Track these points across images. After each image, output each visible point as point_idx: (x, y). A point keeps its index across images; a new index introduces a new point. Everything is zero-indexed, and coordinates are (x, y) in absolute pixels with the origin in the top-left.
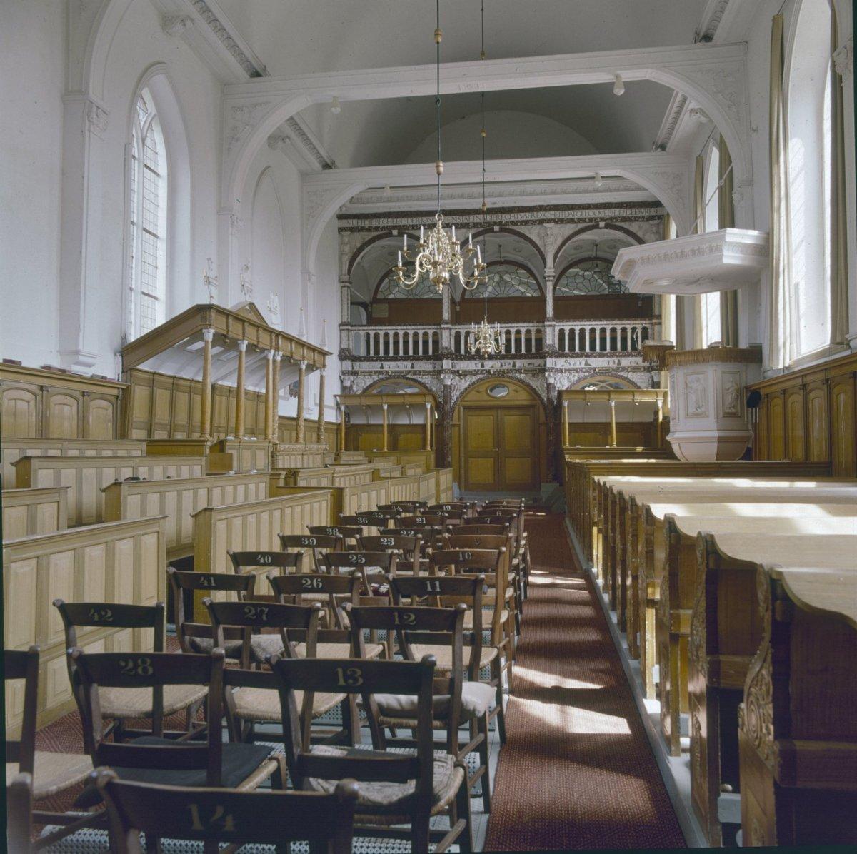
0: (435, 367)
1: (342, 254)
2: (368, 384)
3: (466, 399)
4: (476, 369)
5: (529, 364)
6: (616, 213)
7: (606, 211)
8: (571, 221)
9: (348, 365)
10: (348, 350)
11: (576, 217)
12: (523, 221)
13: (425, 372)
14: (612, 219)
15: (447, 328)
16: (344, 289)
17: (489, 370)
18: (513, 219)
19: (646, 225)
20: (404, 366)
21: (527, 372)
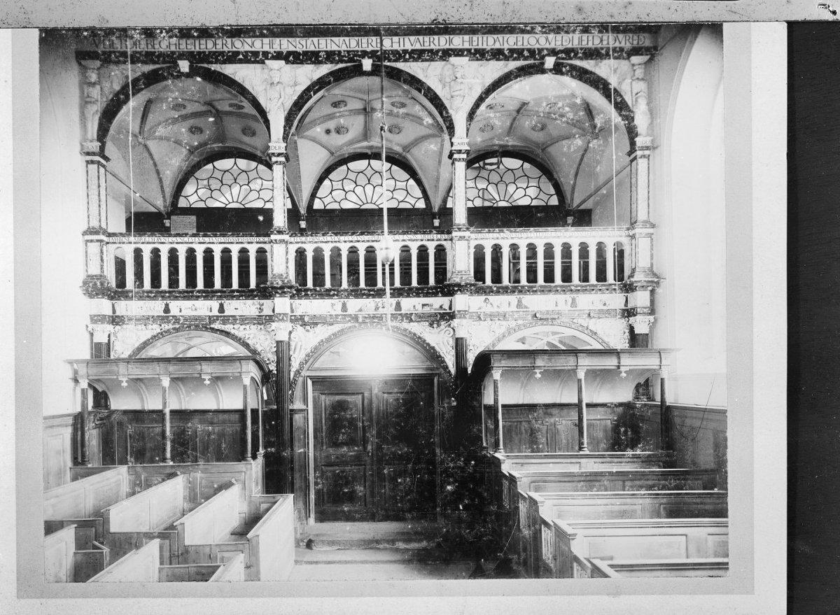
0: (261, 310)
1: (87, 103)
2: (143, 339)
3: (316, 365)
4: (334, 313)
5: (423, 305)
6: (576, 42)
7: (559, 37)
8: (497, 54)
9: (104, 306)
10: (101, 277)
11: (506, 47)
12: (413, 51)
13: (244, 320)
14: (569, 52)
15: (282, 241)
16: (90, 166)
18: (396, 47)
19: (624, 65)
20: (204, 308)
21: (421, 318)
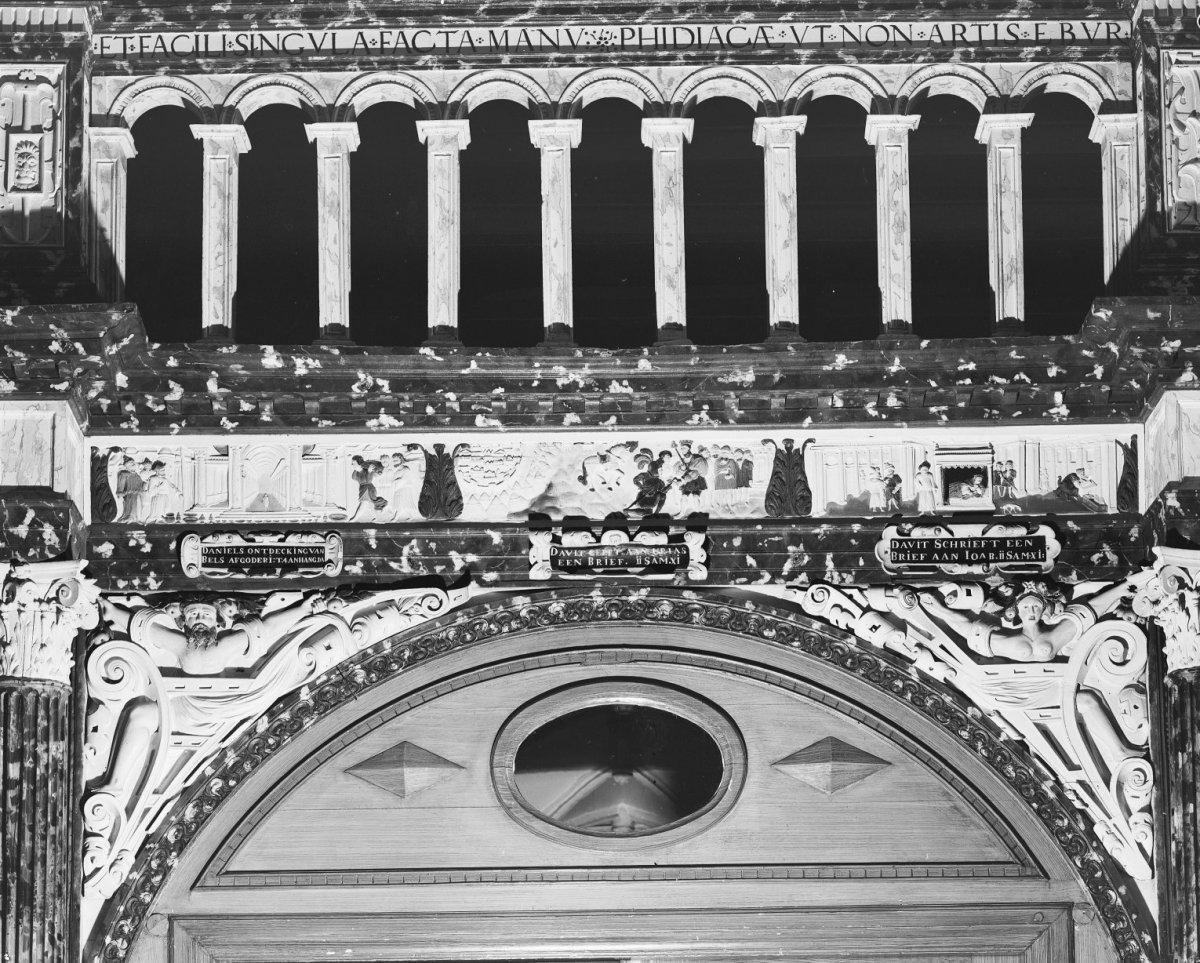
5: (954, 478)
17: (517, 546)
